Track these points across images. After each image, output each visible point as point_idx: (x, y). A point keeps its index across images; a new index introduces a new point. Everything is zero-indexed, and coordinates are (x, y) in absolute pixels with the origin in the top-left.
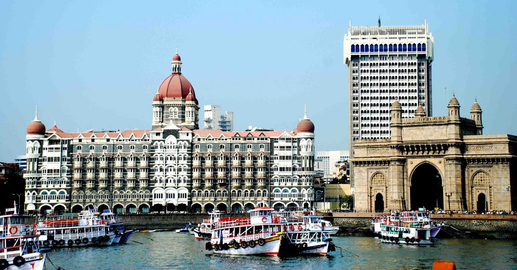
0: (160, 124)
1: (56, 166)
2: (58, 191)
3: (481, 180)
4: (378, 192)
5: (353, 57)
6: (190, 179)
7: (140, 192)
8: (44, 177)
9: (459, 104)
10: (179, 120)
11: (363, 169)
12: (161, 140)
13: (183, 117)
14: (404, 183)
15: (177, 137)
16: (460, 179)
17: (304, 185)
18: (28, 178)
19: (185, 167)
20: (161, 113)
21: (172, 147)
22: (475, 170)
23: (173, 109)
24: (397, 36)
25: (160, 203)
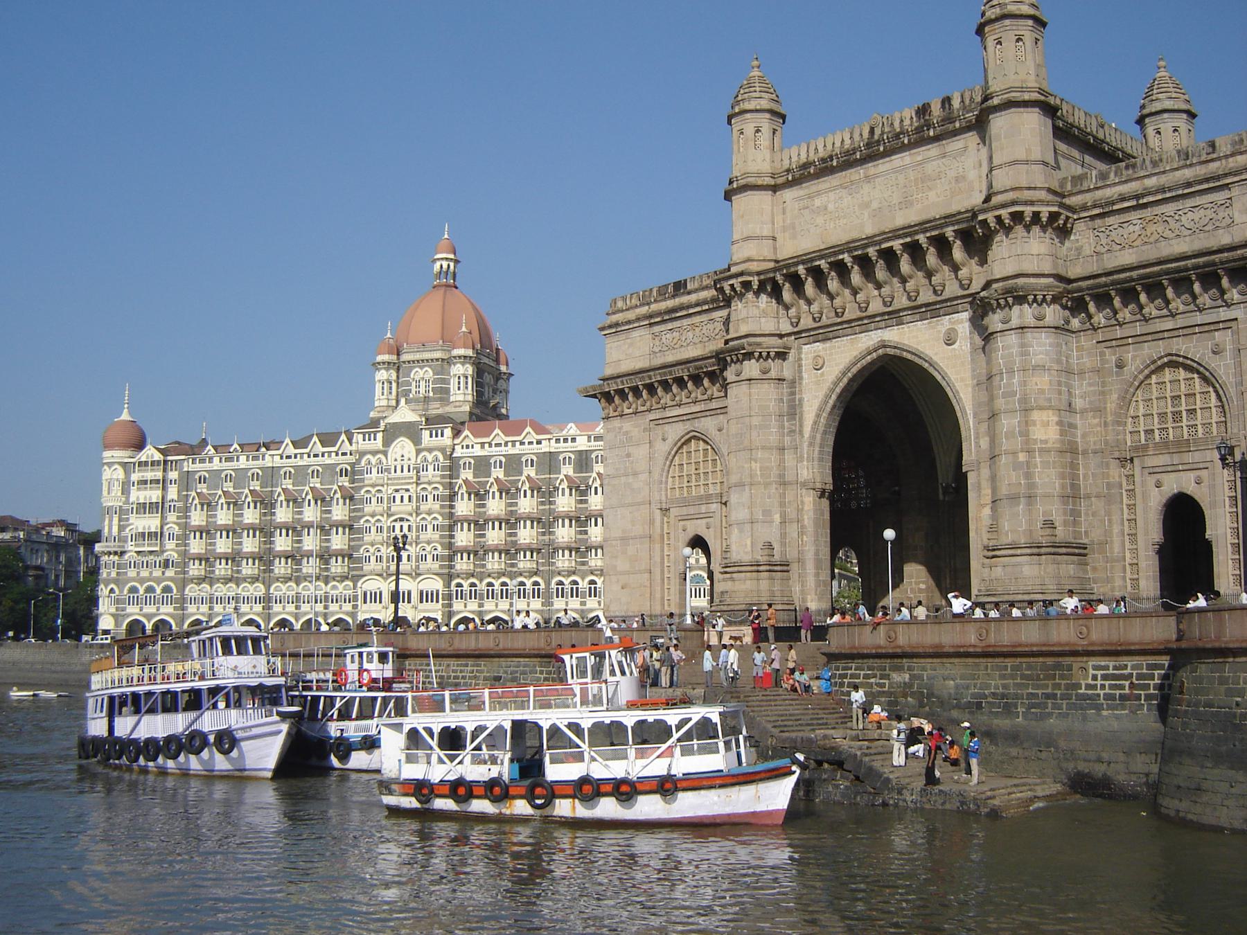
1: (151, 523)
6: (446, 552)
7: (334, 587)
8: (131, 547)
10: (435, 400)
13: (447, 391)
14: (782, 476)
15: (416, 440)
18: (104, 553)
19: (435, 518)
20: (394, 385)
21: (406, 469)
23: (421, 372)
25: (376, 616)
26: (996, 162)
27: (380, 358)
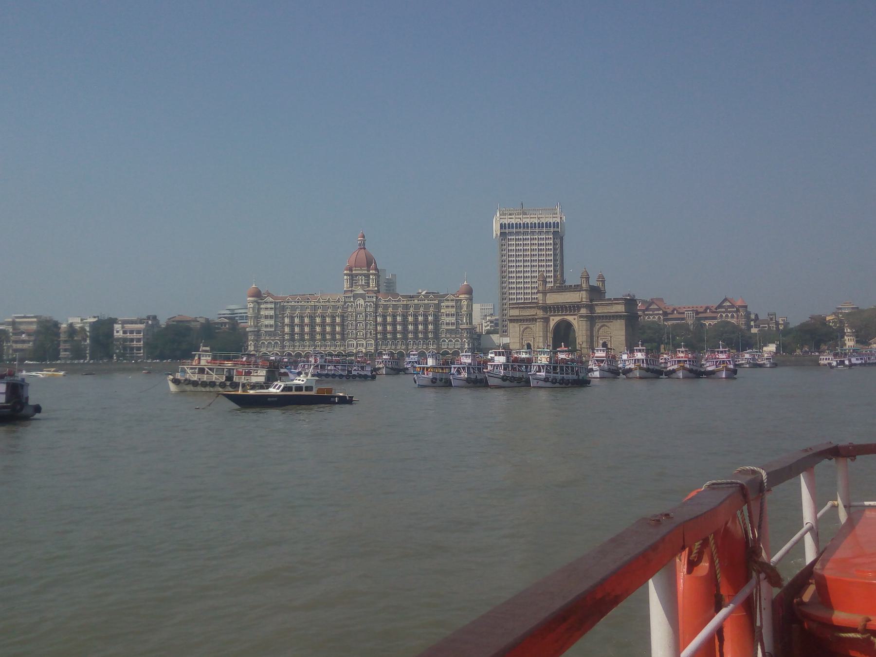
0: (350, 289)
1: (272, 322)
4: (528, 342)
5: (501, 233)
9: (588, 275)
11: (516, 325)
12: (352, 302)
13: (369, 283)
15: (364, 299)
17: (465, 336)
21: (361, 307)
22: (600, 325)
27: (345, 272)
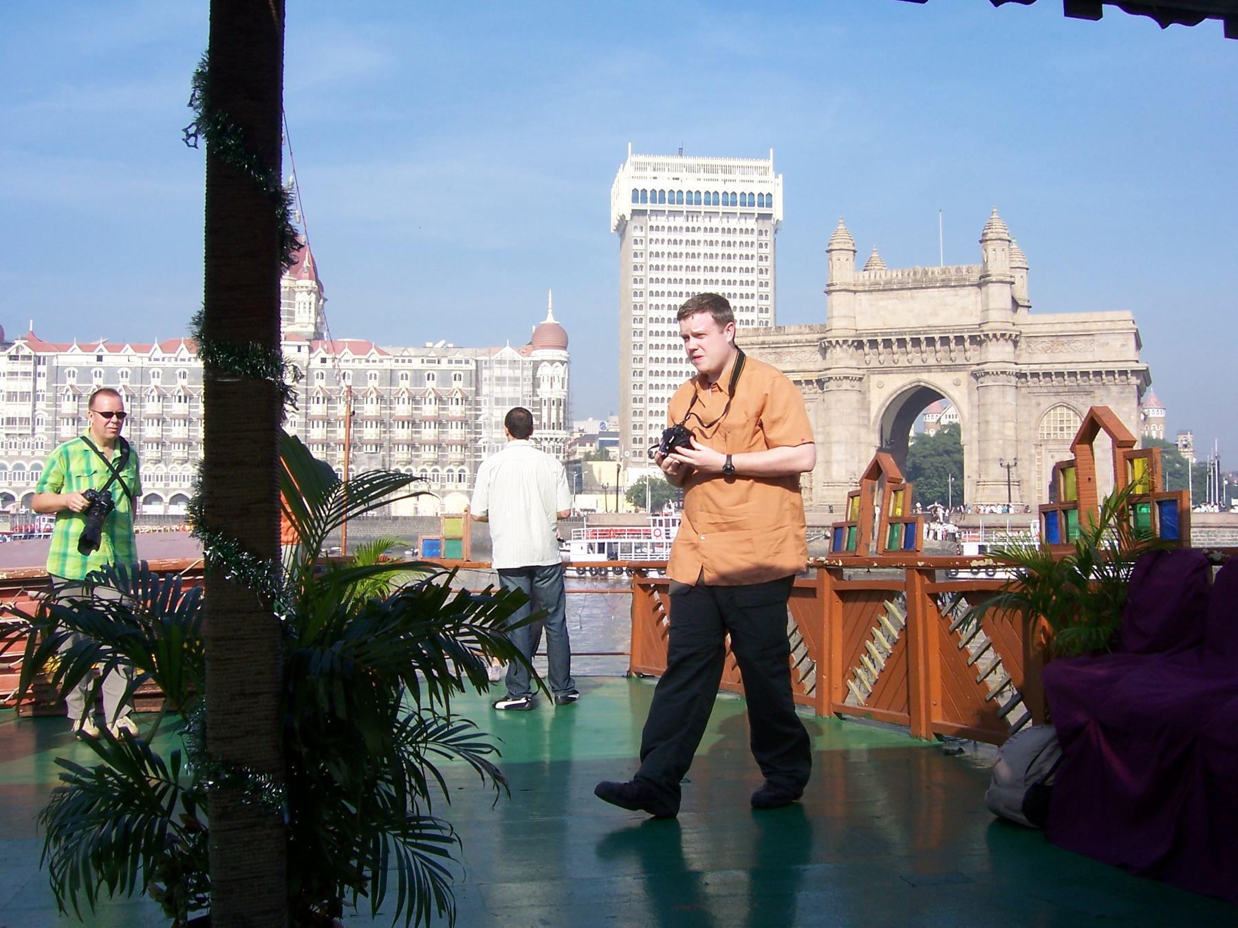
2: (28, 463)
3: (1062, 429)
14: (859, 439)
16: (1011, 425)
24: (721, 176)
26: (991, 306)
